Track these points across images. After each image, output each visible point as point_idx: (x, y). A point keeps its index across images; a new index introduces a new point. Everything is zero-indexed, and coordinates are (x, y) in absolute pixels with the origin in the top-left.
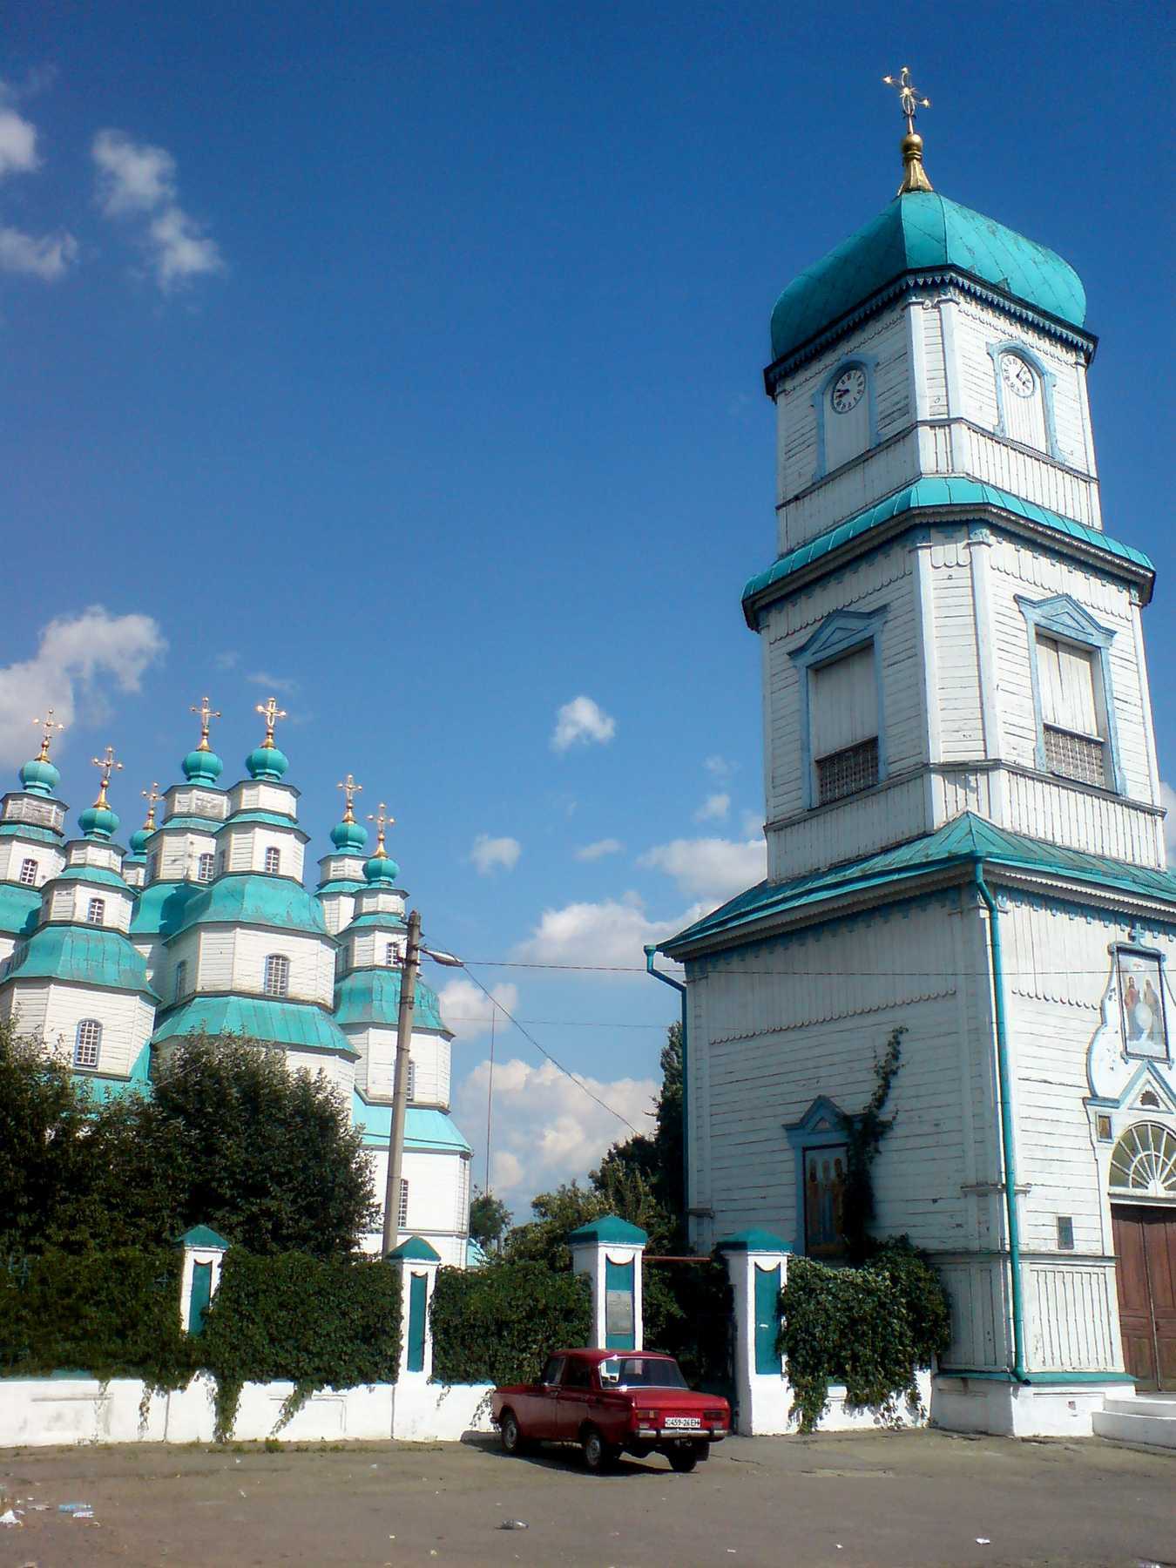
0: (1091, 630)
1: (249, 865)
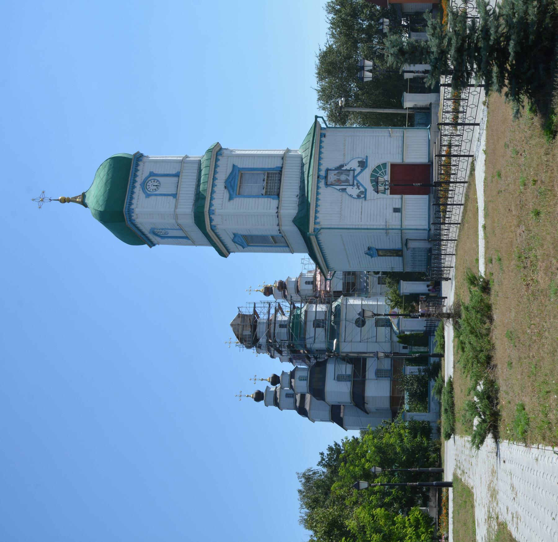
0: (234, 173)
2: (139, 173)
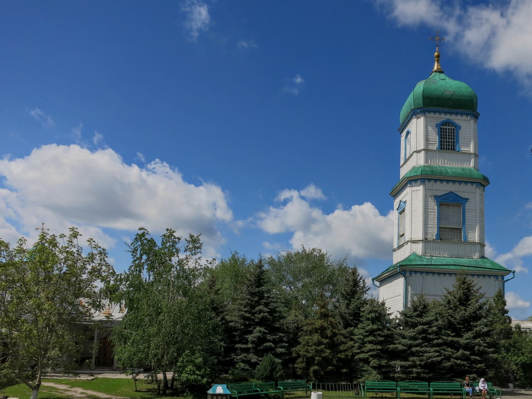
2: (459, 117)
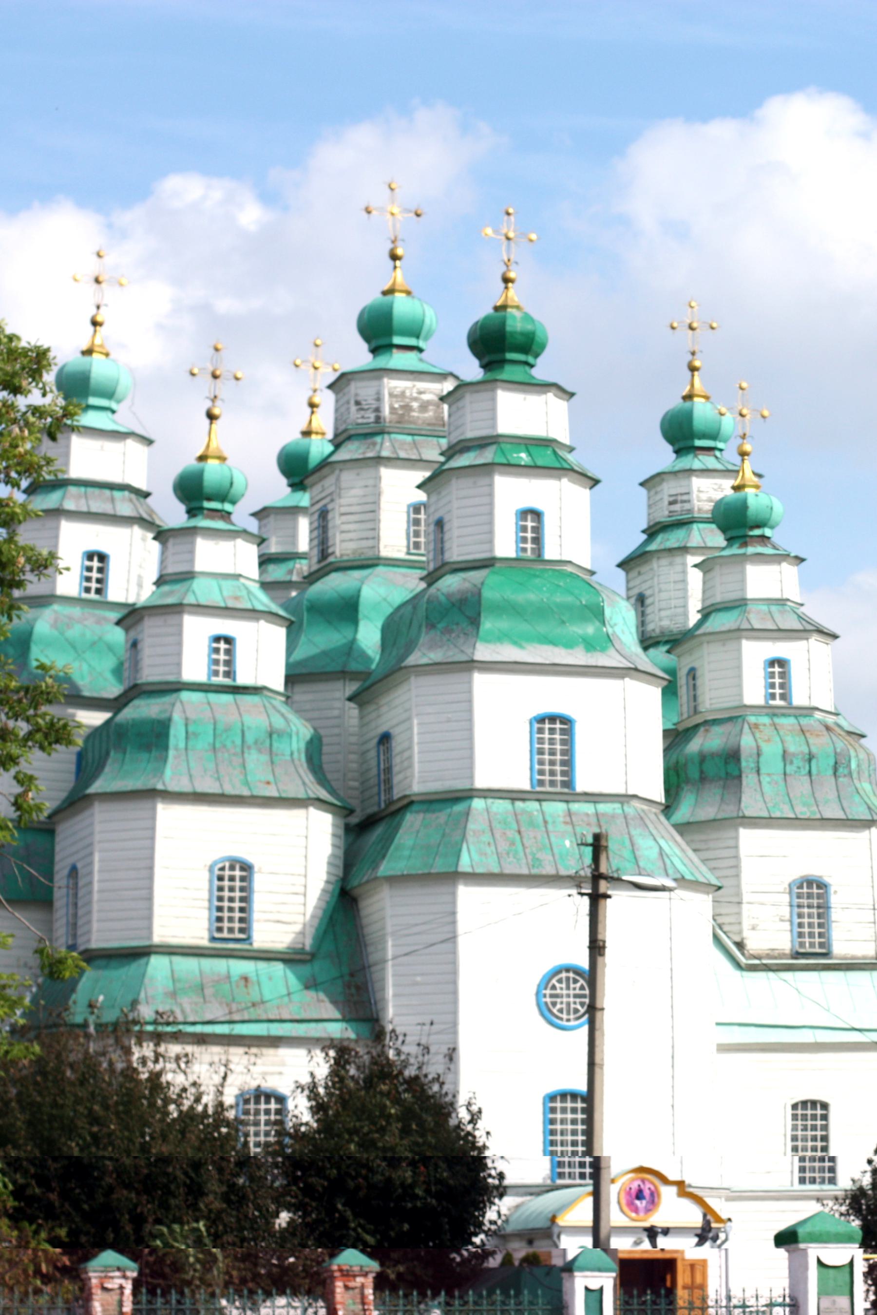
1: (486, 547)
